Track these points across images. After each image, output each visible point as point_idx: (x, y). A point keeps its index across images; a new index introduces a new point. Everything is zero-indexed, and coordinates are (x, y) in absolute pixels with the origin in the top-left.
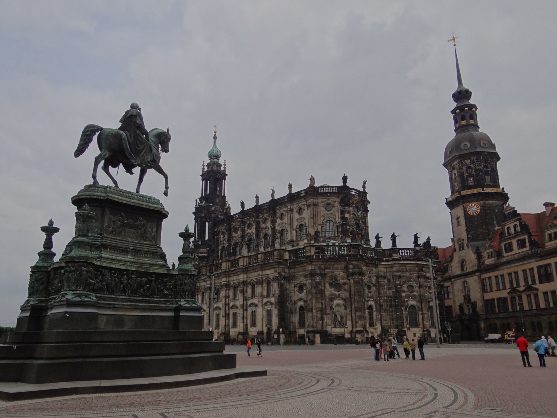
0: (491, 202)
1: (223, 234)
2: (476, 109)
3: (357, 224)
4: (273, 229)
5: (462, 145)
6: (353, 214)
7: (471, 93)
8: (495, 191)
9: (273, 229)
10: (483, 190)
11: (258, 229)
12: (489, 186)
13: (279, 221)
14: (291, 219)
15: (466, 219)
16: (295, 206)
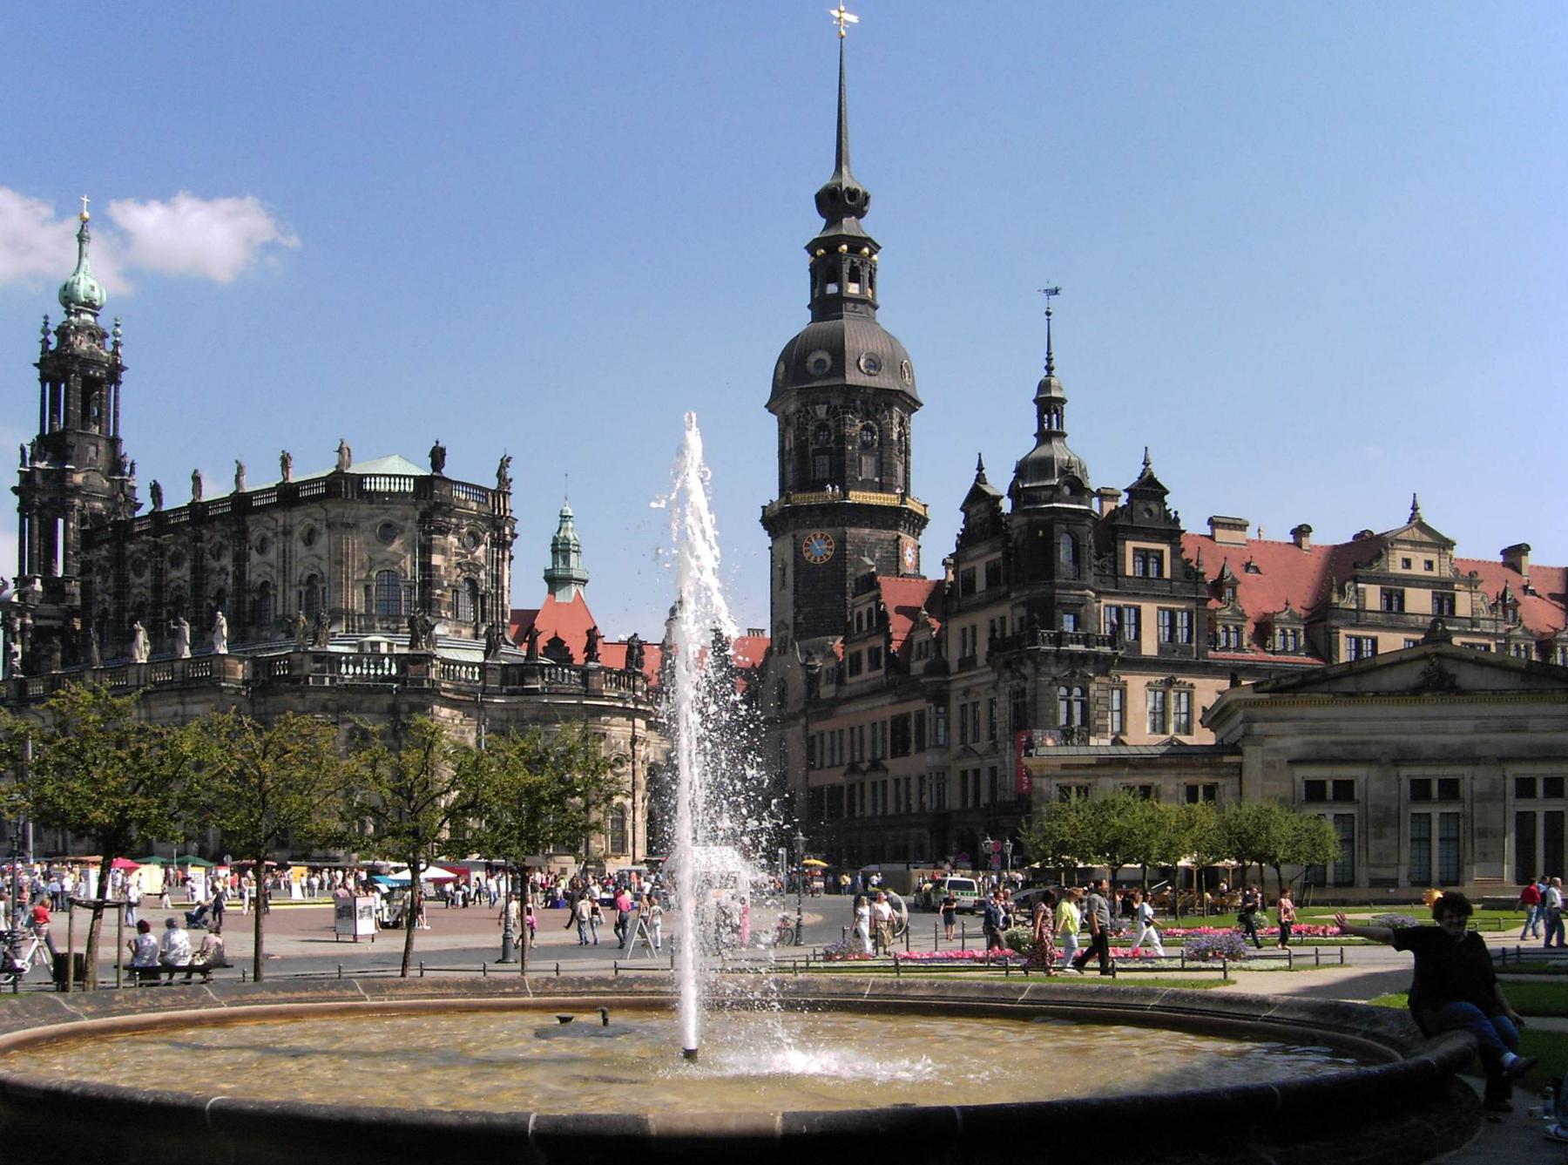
0: (867, 531)
1: (102, 571)
2: (875, 248)
3: (473, 583)
4: (240, 577)
5: (812, 359)
6: (457, 554)
7: (867, 198)
8: (879, 502)
9: (240, 577)
10: (846, 496)
11: (199, 570)
12: (866, 486)
13: (255, 557)
14: (285, 556)
15: (796, 573)
16: (299, 519)
